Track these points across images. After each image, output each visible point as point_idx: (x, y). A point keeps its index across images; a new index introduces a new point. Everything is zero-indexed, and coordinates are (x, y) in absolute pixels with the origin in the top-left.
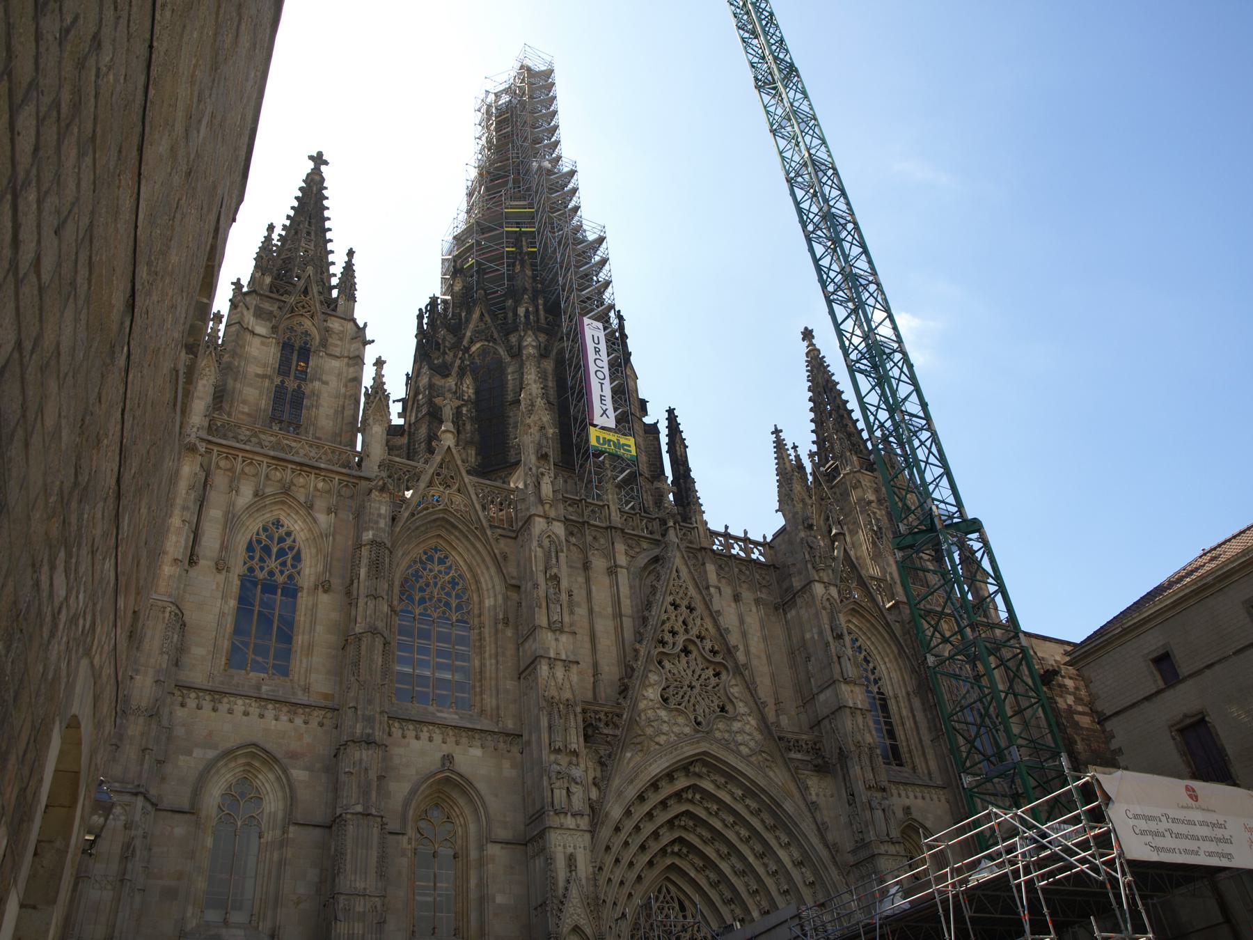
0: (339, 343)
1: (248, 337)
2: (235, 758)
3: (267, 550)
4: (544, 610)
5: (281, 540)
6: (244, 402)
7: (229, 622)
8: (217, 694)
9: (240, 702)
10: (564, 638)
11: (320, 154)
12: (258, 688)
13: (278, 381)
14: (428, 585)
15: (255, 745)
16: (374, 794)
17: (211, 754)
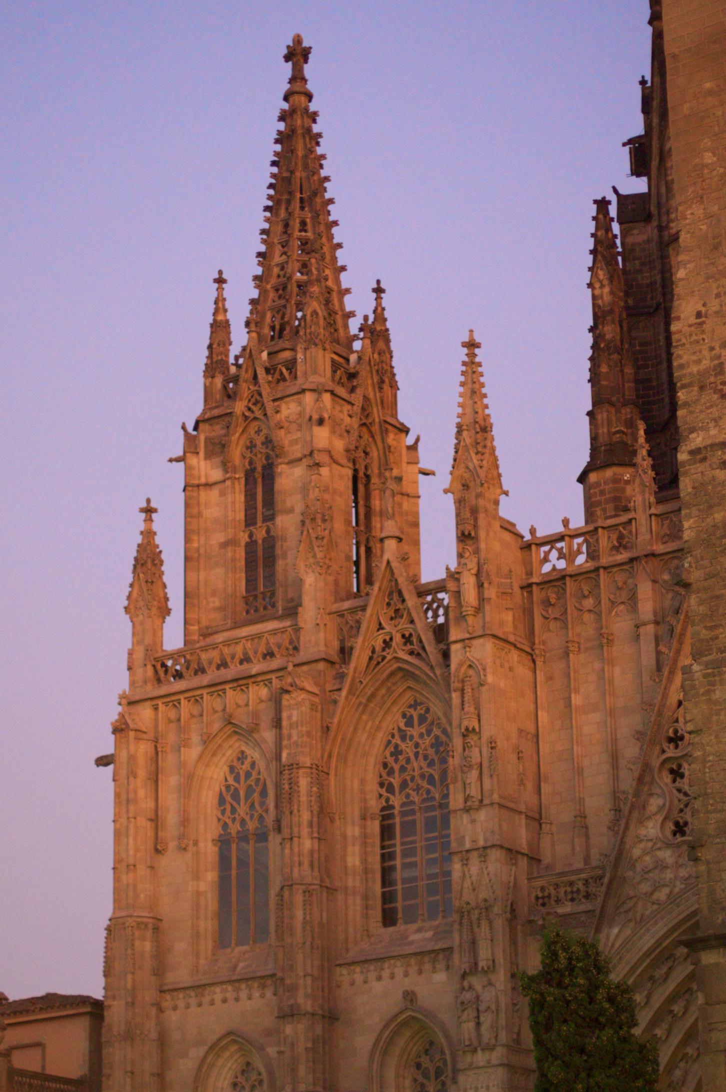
0: (299, 434)
1: (203, 494)
2: (224, 1048)
3: (236, 796)
4: (459, 785)
5: (248, 775)
6: (214, 593)
7: (211, 902)
8: (199, 988)
9: (218, 989)
10: (482, 815)
11: (298, 40)
12: (235, 967)
13: (244, 538)
14: (408, 760)
15: (229, 1033)
16: (302, 1071)
17: (202, 1050)
